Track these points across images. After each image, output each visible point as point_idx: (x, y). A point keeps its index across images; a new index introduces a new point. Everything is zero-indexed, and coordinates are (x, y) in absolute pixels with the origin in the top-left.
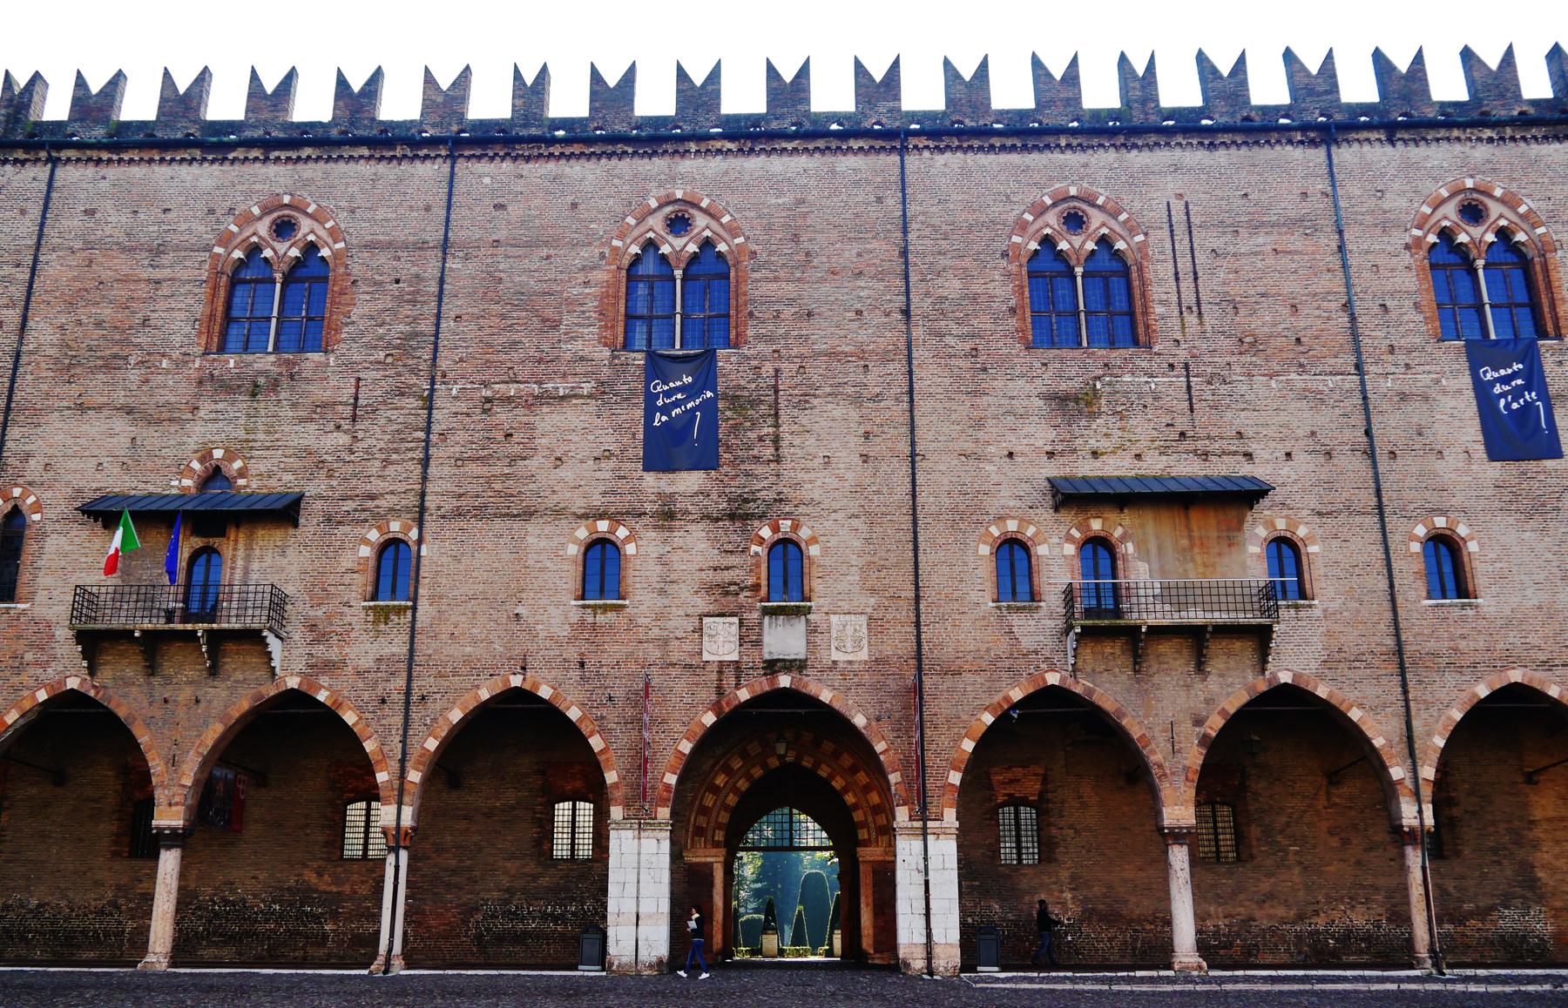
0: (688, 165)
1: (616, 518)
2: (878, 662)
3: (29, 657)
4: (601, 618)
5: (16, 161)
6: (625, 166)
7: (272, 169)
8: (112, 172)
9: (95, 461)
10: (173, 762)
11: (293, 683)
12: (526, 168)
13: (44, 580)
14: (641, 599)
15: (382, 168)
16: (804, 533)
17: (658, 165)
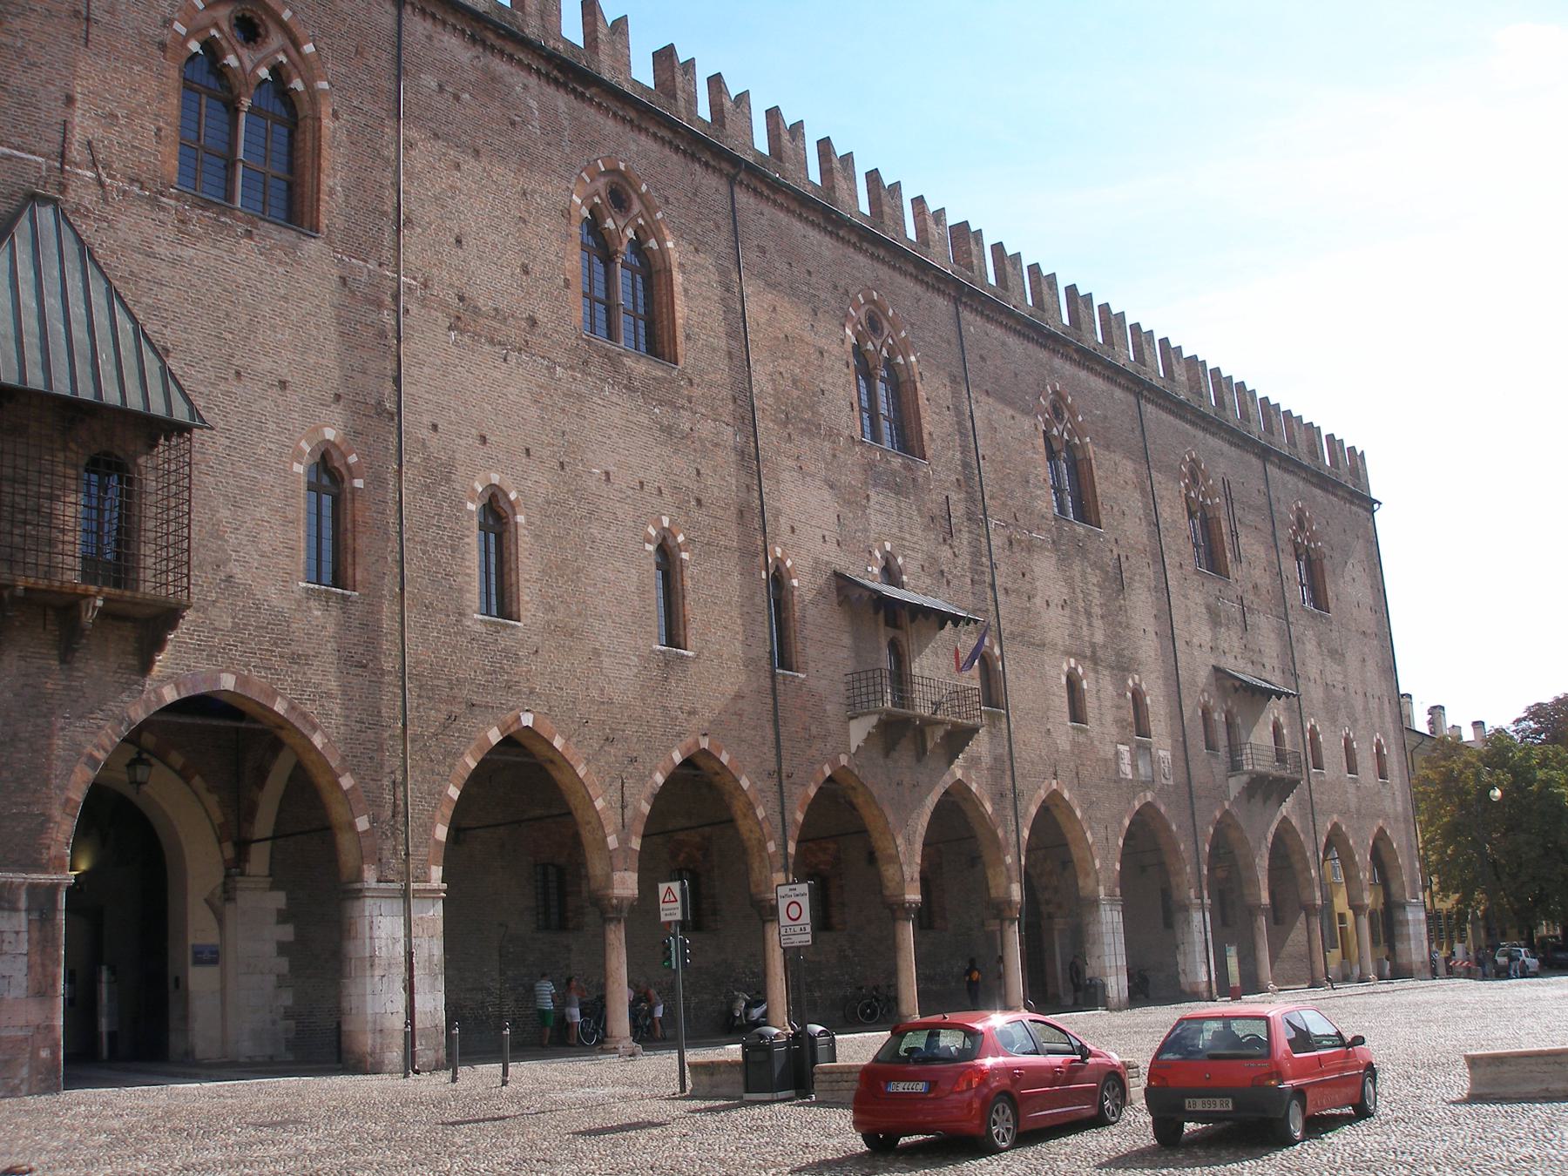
0: (1058, 362)
1: (1080, 657)
2: (1176, 786)
3: (814, 730)
4: (1082, 739)
5: (707, 165)
6: (1032, 349)
7: (861, 260)
8: (768, 210)
9: (819, 532)
10: (909, 842)
11: (959, 774)
12: (990, 327)
13: (812, 652)
14: (1092, 726)
15: (919, 289)
16: (1144, 686)
17: (1043, 355)
